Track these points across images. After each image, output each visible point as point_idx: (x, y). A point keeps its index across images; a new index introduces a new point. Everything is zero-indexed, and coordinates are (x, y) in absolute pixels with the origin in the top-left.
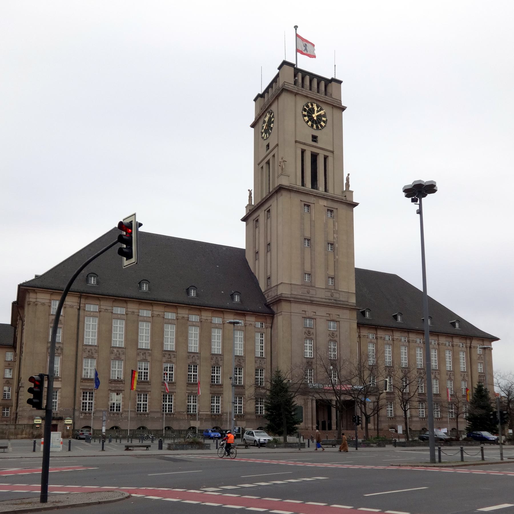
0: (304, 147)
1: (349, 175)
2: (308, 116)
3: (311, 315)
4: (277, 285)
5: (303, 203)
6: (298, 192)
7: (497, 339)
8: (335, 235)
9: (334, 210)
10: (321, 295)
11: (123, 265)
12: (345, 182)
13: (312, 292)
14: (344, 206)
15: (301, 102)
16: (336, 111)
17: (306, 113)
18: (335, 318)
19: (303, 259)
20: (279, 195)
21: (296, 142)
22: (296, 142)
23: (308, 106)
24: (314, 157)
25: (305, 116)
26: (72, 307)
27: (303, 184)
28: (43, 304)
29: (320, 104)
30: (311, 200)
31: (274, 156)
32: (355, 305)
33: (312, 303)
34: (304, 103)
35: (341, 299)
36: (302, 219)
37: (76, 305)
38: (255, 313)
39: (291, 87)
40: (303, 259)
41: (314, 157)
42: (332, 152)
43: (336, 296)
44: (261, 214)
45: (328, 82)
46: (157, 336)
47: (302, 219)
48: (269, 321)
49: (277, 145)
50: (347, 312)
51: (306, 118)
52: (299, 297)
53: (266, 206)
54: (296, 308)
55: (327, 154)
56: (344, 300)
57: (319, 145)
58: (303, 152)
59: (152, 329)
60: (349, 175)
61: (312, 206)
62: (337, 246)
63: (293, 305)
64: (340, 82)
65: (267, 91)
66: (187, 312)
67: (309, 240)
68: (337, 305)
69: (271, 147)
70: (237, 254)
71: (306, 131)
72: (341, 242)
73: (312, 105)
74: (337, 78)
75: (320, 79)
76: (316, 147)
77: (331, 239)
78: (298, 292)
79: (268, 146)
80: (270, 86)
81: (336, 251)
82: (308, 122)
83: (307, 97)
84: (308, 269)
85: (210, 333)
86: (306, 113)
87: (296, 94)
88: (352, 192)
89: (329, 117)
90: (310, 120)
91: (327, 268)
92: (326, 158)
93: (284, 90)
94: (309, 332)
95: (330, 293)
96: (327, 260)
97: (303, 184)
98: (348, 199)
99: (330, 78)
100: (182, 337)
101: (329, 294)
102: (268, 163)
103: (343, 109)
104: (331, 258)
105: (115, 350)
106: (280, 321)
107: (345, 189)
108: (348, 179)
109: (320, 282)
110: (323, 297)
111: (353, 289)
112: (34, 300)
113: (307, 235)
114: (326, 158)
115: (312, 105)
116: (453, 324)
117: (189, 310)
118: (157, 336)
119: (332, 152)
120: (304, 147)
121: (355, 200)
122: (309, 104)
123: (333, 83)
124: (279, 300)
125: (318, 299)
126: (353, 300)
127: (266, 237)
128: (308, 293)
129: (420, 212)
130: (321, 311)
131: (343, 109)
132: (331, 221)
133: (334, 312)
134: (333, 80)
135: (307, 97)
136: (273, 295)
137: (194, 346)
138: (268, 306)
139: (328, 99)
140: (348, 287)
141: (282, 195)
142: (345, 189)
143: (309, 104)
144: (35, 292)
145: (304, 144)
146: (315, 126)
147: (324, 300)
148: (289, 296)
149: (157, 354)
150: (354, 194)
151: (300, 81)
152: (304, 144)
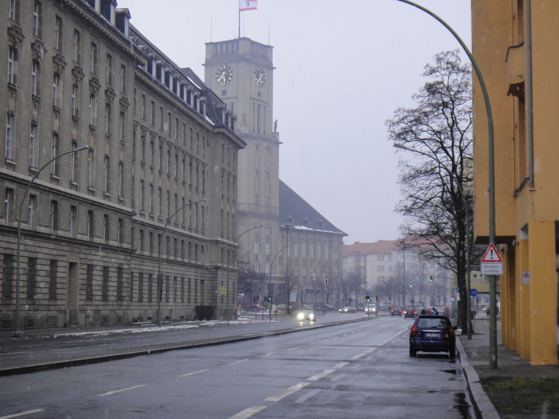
7: (346, 235)
12: (274, 125)
21: (251, 98)
22: (251, 98)
49: (237, 97)
57: (262, 99)
58: (254, 104)
64: (271, 48)
68: (269, 216)
76: (260, 100)
99: (267, 44)
108: (276, 123)
119: (268, 103)
126: (278, 213)
140: (275, 203)
150: (280, 135)
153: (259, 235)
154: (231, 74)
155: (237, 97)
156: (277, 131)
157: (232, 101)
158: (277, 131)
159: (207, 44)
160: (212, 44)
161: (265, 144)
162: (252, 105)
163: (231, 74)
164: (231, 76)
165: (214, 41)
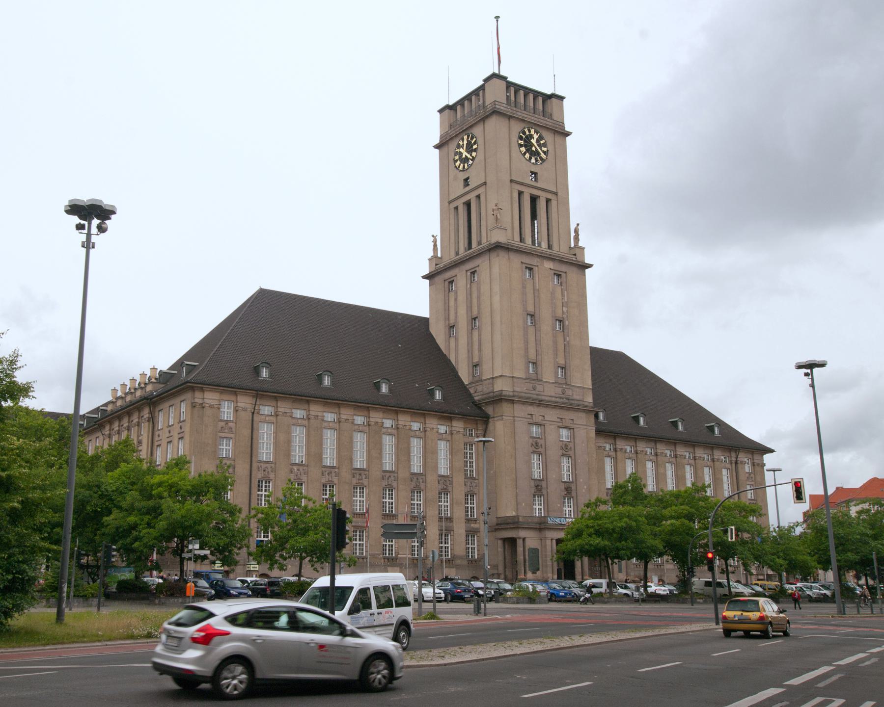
0: (522, 188)
1: (578, 225)
2: (525, 146)
3: (539, 419)
4: (493, 378)
5: (524, 266)
6: (518, 251)
8: (565, 309)
9: (563, 275)
10: (550, 392)
11: (279, 348)
12: (573, 234)
13: (539, 388)
14: (575, 269)
15: (517, 127)
16: (558, 138)
17: (522, 142)
18: (568, 423)
19: (526, 342)
20: (493, 255)
21: (512, 181)
22: (512, 181)
23: (524, 133)
24: (534, 200)
25: (521, 146)
26: (245, 410)
27: (522, 240)
28: (211, 406)
29: (538, 129)
30: (534, 261)
31: (478, 197)
32: (592, 405)
33: (540, 403)
34: (520, 129)
35: (575, 397)
36: (524, 287)
37: (250, 407)
38: (464, 416)
39: (502, 108)
40: (526, 342)
41: (534, 200)
42: (556, 194)
43: (569, 392)
44: (461, 276)
45: (547, 98)
46: (345, 448)
47: (524, 287)
48: (481, 427)
49: (485, 183)
50: (583, 415)
51: (523, 149)
52: (524, 395)
53: (470, 265)
54: (521, 411)
55: (549, 196)
56: (578, 398)
58: (520, 193)
59: (339, 439)
60: (578, 225)
61: (535, 269)
62: (567, 323)
63: (517, 407)
65: (461, 102)
66: (381, 415)
67: (532, 316)
68: (567, 405)
69: (473, 183)
70: (416, 327)
71: (523, 166)
72: (571, 318)
73: (529, 131)
74: (558, 93)
75: (537, 94)
77: (559, 314)
78: (522, 388)
79: (466, 180)
80: (468, 97)
81: (566, 331)
82: (525, 154)
83: (523, 121)
84: (532, 356)
85: (409, 443)
86: (522, 142)
87: (510, 117)
88: (583, 249)
89: (550, 147)
90: (527, 151)
91: (556, 355)
92: (548, 201)
93: (495, 112)
94: (537, 443)
95: (560, 389)
96: (555, 343)
97: (522, 240)
98: (578, 259)
99: (549, 93)
100: (375, 449)
101: (559, 390)
102: (468, 204)
103: (568, 134)
104: (560, 340)
105: (295, 468)
106: (499, 427)
107: (572, 245)
108: (576, 231)
109: (548, 374)
110: (553, 394)
111: (589, 383)
112: (200, 401)
113: (531, 309)
114: (548, 201)
115: (529, 131)
116: (711, 429)
117: (384, 412)
118: (345, 448)
119: (556, 194)
120: (522, 188)
121: (587, 261)
122: (526, 130)
123: (554, 100)
124: (499, 399)
125: (547, 398)
126: (589, 399)
127: (470, 308)
128: (534, 389)
129: (812, 385)
130: (552, 415)
131: (568, 134)
132: (558, 290)
133: (568, 415)
134: (553, 96)
135: (523, 121)
136: (486, 390)
137: (388, 462)
138: (477, 405)
139: (548, 122)
140: (582, 378)
141: (498, 256)
142: (572, 245)
143: (526, 130)
144: (202, 390)
145: (522, 184)
146: (533, 160)
147: (554, 399)
148: (511, 394)
149: (345, 474)
150: (587, 253)
151: (513, 98)
152: (522, 184)
153: (541, 442)
154: (475, 147)
155: (485, 183)
156: (580, 244)
157: (476, 193)
158: (580, 244)
159: (441, 111)
160: (448, 107)
161: (549, 265)
162: (516, 195)
163: (475, 147)
164: (475, 150)
165: (451, 104)
